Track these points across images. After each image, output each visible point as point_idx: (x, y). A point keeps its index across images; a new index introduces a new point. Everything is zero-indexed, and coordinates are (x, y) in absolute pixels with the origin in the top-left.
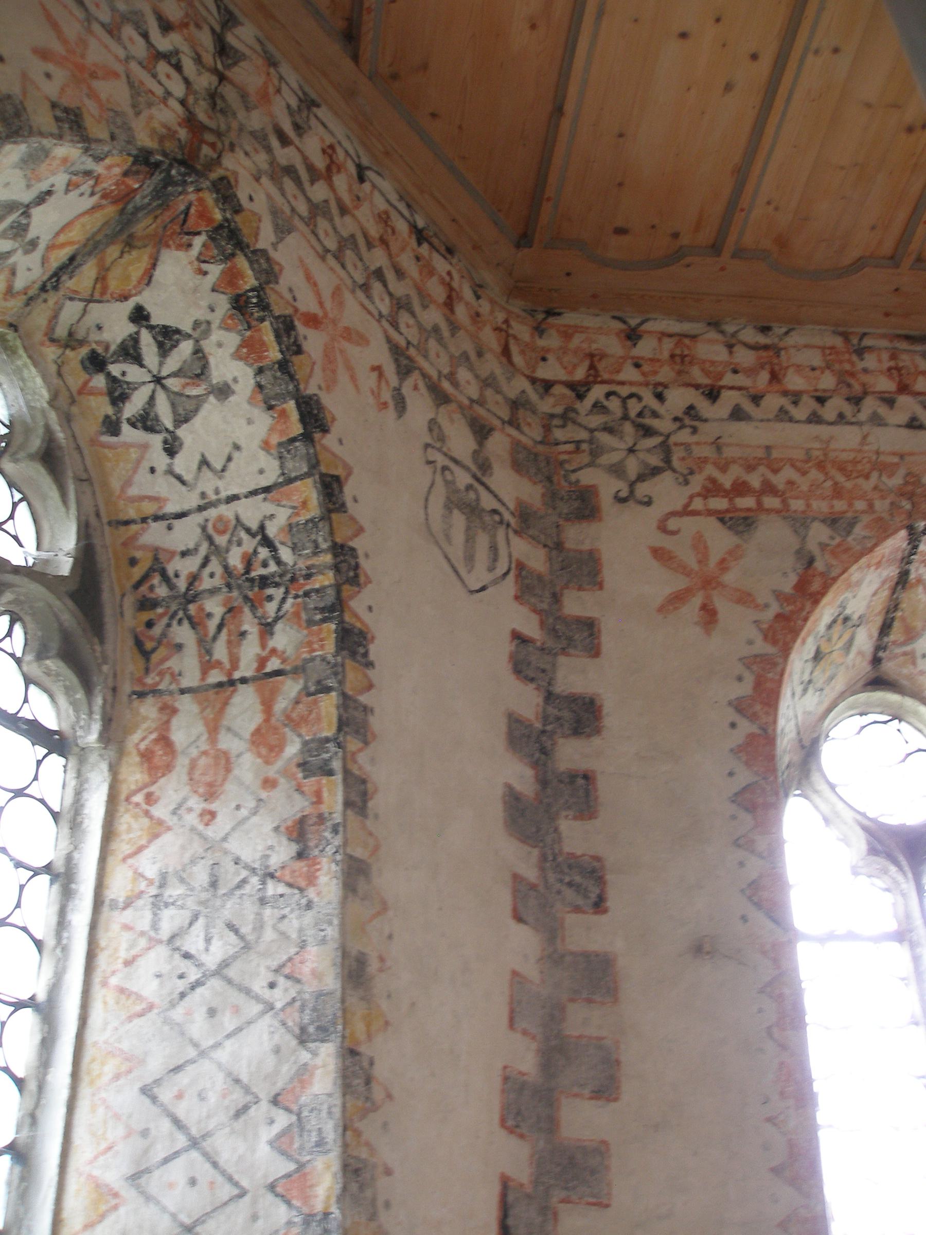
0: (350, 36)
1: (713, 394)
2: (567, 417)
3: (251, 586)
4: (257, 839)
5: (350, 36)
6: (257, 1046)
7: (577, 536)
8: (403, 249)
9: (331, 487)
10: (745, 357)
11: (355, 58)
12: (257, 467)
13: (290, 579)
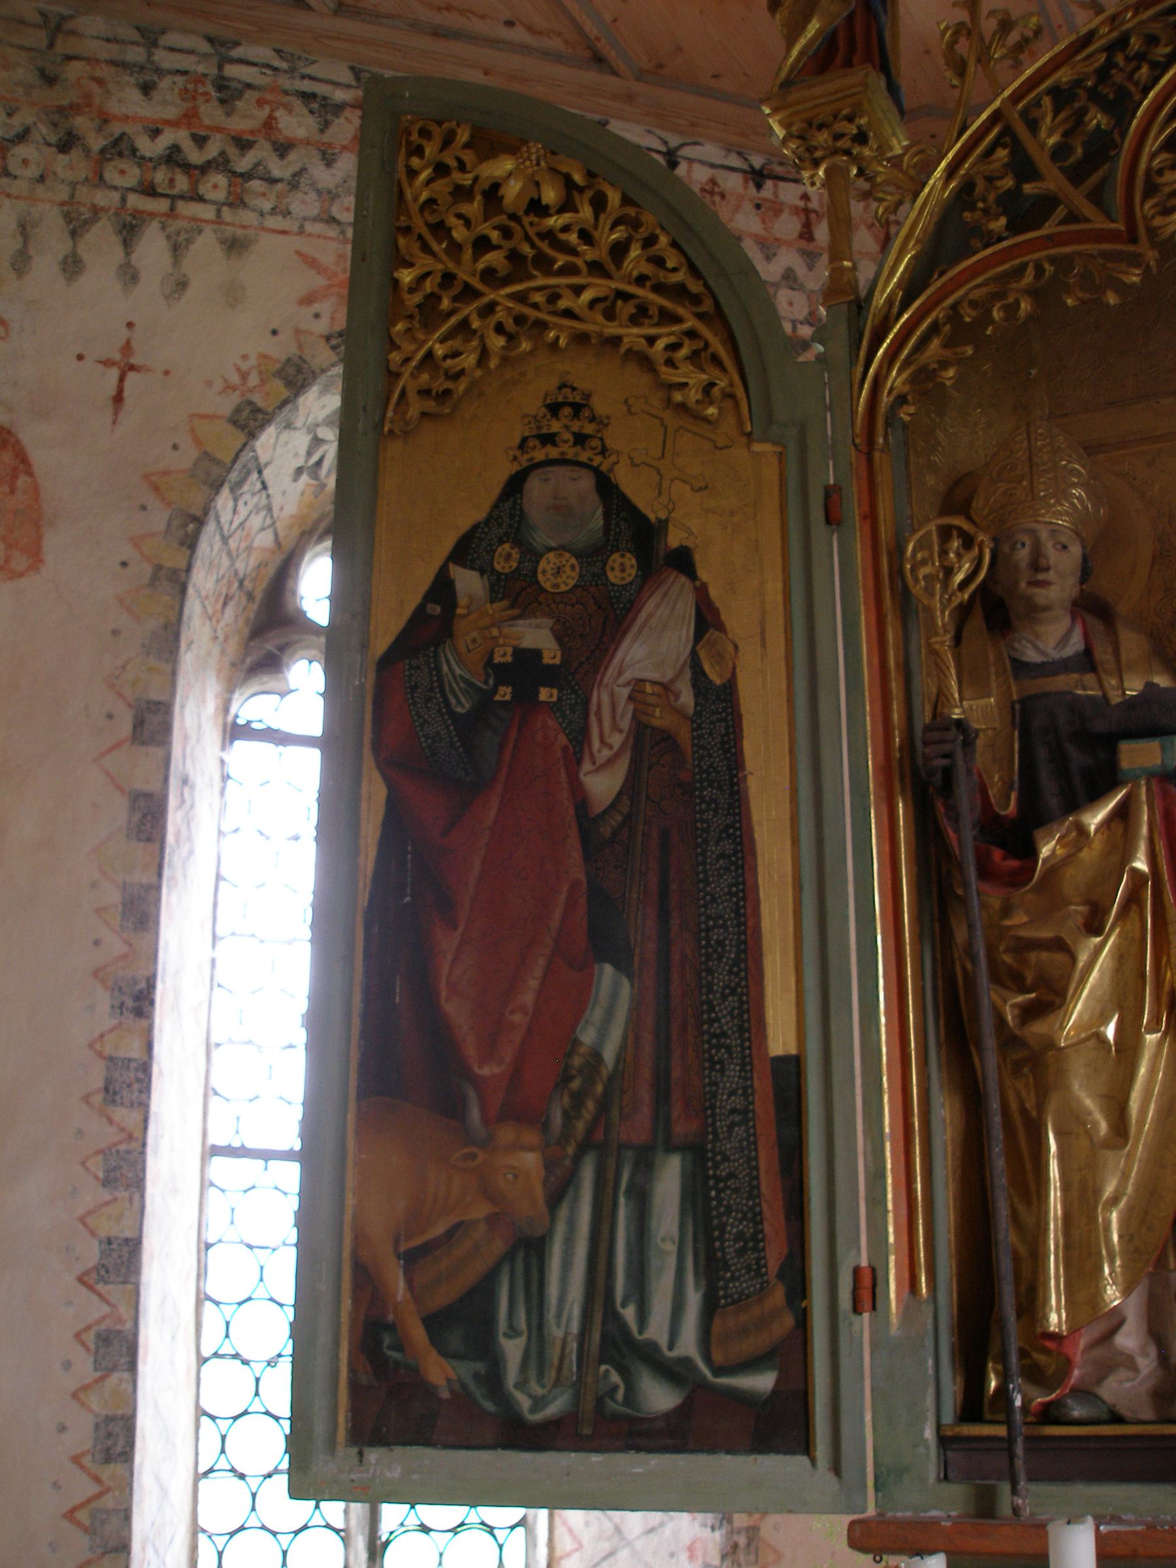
0: (598, 60)
5: (598, 60)
8: (737, 208)
11: (615, 73)
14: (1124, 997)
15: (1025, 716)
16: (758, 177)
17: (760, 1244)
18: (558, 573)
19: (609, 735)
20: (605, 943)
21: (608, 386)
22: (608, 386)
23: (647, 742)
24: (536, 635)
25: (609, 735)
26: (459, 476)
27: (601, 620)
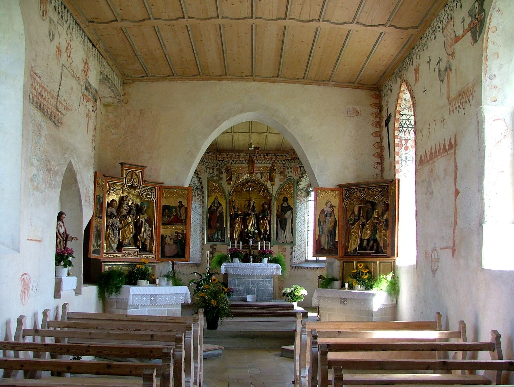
1: (233, 161)
2: (221, 164)
3: (197, 189)
4: (198, 205)
6: (198, 216)
7: (221, 176)
9: (201, 183)
10: (237, 157)
12: (196, 182)
13: (199, 189)
16: (208, 153)
17: (223, 234)
18: (216, 205)
19: (218, 213)
21: (219, 196)
22: (218, 195)
24: (215, 208)
25: (218, 213)
26: (212, 200)
27: (218, 208)
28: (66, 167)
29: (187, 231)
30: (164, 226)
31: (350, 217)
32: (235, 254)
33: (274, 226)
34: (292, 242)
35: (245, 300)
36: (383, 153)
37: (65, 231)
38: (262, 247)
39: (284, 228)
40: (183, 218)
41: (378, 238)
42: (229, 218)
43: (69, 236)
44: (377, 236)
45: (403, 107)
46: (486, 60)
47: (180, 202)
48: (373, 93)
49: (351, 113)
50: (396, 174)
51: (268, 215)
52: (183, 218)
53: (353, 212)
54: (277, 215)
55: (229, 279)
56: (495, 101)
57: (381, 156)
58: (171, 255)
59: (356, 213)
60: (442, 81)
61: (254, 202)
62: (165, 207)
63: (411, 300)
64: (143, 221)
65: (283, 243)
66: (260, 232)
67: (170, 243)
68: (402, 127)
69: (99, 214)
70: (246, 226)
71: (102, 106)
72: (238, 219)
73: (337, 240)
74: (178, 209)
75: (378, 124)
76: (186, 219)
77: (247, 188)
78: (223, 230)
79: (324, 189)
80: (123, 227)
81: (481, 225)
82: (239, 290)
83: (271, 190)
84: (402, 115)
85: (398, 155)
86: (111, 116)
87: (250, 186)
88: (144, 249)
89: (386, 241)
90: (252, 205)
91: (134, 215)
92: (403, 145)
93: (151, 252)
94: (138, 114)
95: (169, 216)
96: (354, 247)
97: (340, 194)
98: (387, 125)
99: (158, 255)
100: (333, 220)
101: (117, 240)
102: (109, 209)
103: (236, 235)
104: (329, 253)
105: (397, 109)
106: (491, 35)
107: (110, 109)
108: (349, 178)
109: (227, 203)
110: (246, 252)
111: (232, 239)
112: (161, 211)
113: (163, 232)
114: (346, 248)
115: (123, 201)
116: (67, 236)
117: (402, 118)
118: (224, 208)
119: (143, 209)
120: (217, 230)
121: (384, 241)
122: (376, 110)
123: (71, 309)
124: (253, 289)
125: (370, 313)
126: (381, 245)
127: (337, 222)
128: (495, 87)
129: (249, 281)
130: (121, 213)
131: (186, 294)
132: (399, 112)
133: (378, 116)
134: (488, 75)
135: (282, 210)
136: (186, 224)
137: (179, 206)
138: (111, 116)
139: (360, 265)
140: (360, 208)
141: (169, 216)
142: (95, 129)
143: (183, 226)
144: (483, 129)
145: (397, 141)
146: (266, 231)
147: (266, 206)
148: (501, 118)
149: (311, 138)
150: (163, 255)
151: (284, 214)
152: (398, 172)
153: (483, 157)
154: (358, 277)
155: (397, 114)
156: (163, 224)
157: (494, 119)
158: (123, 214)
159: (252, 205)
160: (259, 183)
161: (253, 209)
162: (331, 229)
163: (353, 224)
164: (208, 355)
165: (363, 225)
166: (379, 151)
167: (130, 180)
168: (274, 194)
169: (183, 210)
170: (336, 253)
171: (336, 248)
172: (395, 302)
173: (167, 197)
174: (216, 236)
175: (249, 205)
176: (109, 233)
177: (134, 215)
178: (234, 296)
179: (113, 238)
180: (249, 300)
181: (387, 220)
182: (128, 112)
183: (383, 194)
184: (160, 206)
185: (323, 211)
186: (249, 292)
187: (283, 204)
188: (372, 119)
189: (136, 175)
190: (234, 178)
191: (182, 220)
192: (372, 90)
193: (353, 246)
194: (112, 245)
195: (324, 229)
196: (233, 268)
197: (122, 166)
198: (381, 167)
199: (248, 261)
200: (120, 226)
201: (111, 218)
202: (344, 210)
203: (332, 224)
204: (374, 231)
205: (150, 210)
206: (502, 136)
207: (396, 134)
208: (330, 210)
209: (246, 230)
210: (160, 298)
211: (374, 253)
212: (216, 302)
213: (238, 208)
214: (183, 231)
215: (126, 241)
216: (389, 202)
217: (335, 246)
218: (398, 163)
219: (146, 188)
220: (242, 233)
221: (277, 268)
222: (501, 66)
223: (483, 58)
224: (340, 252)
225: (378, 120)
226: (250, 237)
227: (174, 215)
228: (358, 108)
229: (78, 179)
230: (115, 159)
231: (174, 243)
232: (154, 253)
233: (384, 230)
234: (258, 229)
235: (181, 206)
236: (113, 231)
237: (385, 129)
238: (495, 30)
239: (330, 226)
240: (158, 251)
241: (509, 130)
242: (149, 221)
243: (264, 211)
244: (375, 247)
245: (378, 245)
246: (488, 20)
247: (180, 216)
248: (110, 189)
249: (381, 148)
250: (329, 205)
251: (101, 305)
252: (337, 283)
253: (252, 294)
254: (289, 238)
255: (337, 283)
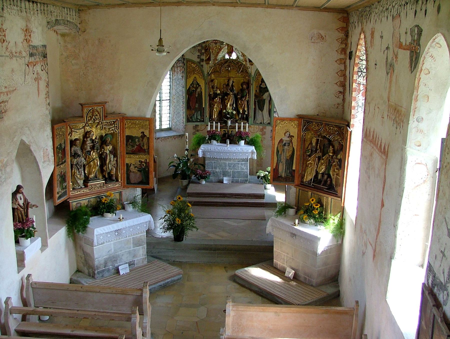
4: (180, 77)
6: (181, 88)
14: (217, 106)
15: (214, 93)
17: (202, 115)
18: (195, 86)
19: (197, 93)
20: (197, 102)
21: (197, 77)
23: (199, 94)
24: (194, 89)
25: (197, 93)
26: (190, 81)
27: (197, 88)
28: (16, 151)
29: (150, 160)
30: (127, 156)
31: (308, 147)
32: (212, 136)
33: (252, 106)
34: (269, 123)
35: (221, 181)
36: (344, 87)
37: (25, 200)
38: (239, 128)
39: (261, 109)
40: (145, 147)
41: (331, 175)
42: (208, 98)
43: (30, 204)
44: (331, 173)
45: (363, 53)
46: (416, 100)
47: (143, 133)
48: (340, 16)
49: (315, 38)
50: (352, 120)
51: (246, 95)
52: (145, 147)
53: (311, 143)
54: (255, 95)
55: (206, 162)
56: (419, 146)
57: (343, 85)
58: (136, 182)
59: (314, 144)
60: (388, 74)
61: (233, 82)
62: (129, 138)
63: (350, 253)
64: (108, 152)
65: (261, 123)
66: (238, 112)
67: (134, 171)
68: (362, 71)
69: (63, 160)
70: (225, 107)
71: (59, 37)
72: (217, 100)
73: (294, 168)
74: (141, 139)
75: (344, 51)
76: (148, 149)
77: (225, 68)
78: (202, 110)
79: (283, 120)
80: (89, 163)
81: (391, 258)
82: (216, 172)
83: (250, 70)
84: (362, 60)
85: (355, 100)
86: (69, 46)
87: (229, 66)
88: (109, 178)
89: (339, 179)
90: (230, 85)
91: (97, 150)
92: (360, 91)
93: (117, 181)
94: (97, 42)
95: (133, 146)
96: (309, 178)
97: (299, 125)
98: (350, 58)
99: (124, 183)
100: (292, 149)
101: (83, 176)
102: (73, 149)
103: (215, 116)
104: (286, 181)
105: (357, 54)
106: (423, 76)
107: (68, 39)
108: (309, 108)
109: (206, 84)
110: (225, 131)
111: (211, 119)
112: (125, 141)
113: (127, 161)
114: (303, 177)
115: (87, 139)
116: (28, 203)
117: (361, 63)
118: (203, 88)
119: (106, 141)
120: (196, 110)
121: (337, 179)
122: (342, 35)
123: (35, 279)
124: (229, 171)
125: (315, 253)
126: (334, 183)
127: (295, 151)
128: (421, 131)
129: (225, 164)
130: (85, 149)
131: (150, 221)
132: (359, 57)
133: (344, 42)
134: (416, 117)
135: (260, 91)
136: (149, 154)
137: (142, 136)
138: (69, 46)
139: (313, 200)
140: (318, 140)
141: (133, 146)
142: (47, 86)
143: (147, 156)
144: (405, 169)
145: (355, 85)
146: (244, 110)
147: (245, 86)
148: (424, 162)
149: (272, 65)
150: (129, 183)
151: (263, 95)
152: (354, 118)
153: (402, 196)
154: (309, 212)
155: (356, 59)
156: (127, 153)
157: (417, 162)
158: (87, 150)
159: (230, 85)
160: (238, 63)
161: (232, 90)
162: (288, 158)
163: (310, 156)
164: (168, 282)
165: (319, 158)
166: (342, 79)
167: (91, 118)
168: (253, 74)
169: (145, 140)
170: (294, 181)
171: (293, 177)
172: (340, 242)
173: (129, 128)
174: (195, 116)
175: (228, 85)
176: (74, 171)
177: (97, 150)
178: (212, 178)
179: (79, 176)
180: (225, 182)
181: (340, 160)
182: (87, 41)
183: (339, 134)
184: (123, 136)
185: (281, 141)
186: (225, 174)
187: (261, 84)
188: (337, 45)
189: (97, 111)
190: (212, 58)
191: (145, 150)
192: (340, 13)
193: (309, 177)
194: (79, 182)
195: (282, 157)
196: (210, 152)
197: (82, 107)
198: (343, 96)
199: (225, 143)
200: (85, 163)
201: (75, 158)
202: (302, 140)
203: (290, 153)
204: (328, 167)
205: (114, 140)
206: (422, 181)
207: (355, 78)
208: (288, 139)
209: (225, 111)
210: (124, 232)
211: (327, 189)
212: (180, 221)
213: (217, 87)
214: (146, 160)
215: (92, 176)
216: (343, 144)
217: (292, 175)
218: (354, 109)
219: (108, 121)
220: (220, 113)
221: (252, 153)
222: (430, 111)
223: (414, 97)
224: (297, 181)
225: (343, 46)
226: (228, 118)
227: (137, 145)
228: (323, 33)
229: (32, 150)
230: (77, 90)
231: (138, 171)
232: (120, 180)
233: (337, 169)
234: (237, 109)
235: (143, 136)
236: (79, 169)
237: (348, 60)
238: (427, 72)
239: (288, 155)
240: (124, 178)
241: (429, 176)
242: (114, 152)
243: (242, 90)
244: (329, 182)
245: (331, 181)
246: (421, 61)
247: (143, 146)
248: (71, 130)
249: (345, 76)
250: (287, 134)
251: (72, 241)
252: (291, 212)
253: (229, 176)
254: (266, 120)
255: (291, 212)
